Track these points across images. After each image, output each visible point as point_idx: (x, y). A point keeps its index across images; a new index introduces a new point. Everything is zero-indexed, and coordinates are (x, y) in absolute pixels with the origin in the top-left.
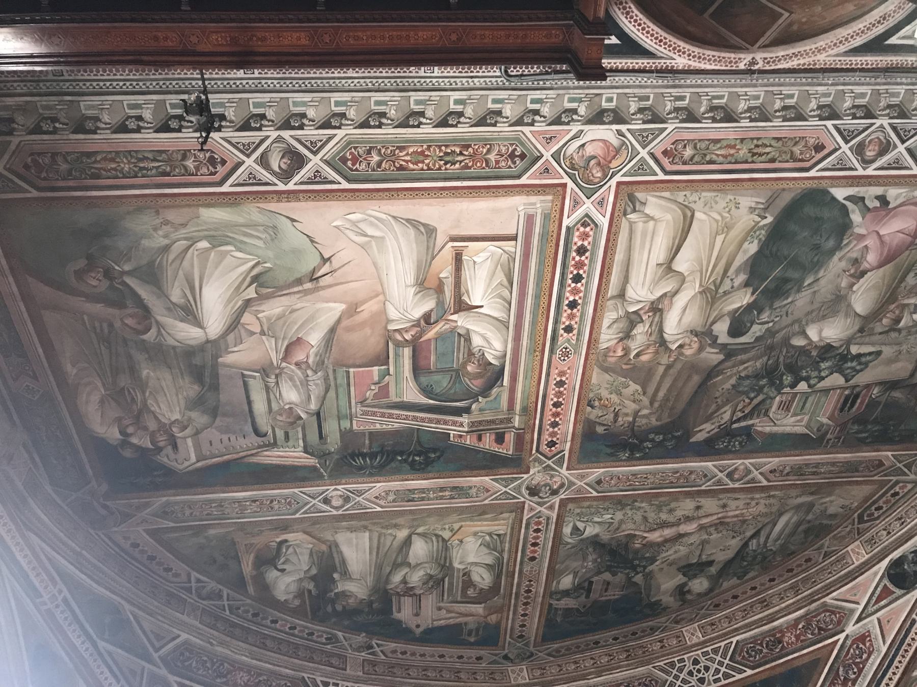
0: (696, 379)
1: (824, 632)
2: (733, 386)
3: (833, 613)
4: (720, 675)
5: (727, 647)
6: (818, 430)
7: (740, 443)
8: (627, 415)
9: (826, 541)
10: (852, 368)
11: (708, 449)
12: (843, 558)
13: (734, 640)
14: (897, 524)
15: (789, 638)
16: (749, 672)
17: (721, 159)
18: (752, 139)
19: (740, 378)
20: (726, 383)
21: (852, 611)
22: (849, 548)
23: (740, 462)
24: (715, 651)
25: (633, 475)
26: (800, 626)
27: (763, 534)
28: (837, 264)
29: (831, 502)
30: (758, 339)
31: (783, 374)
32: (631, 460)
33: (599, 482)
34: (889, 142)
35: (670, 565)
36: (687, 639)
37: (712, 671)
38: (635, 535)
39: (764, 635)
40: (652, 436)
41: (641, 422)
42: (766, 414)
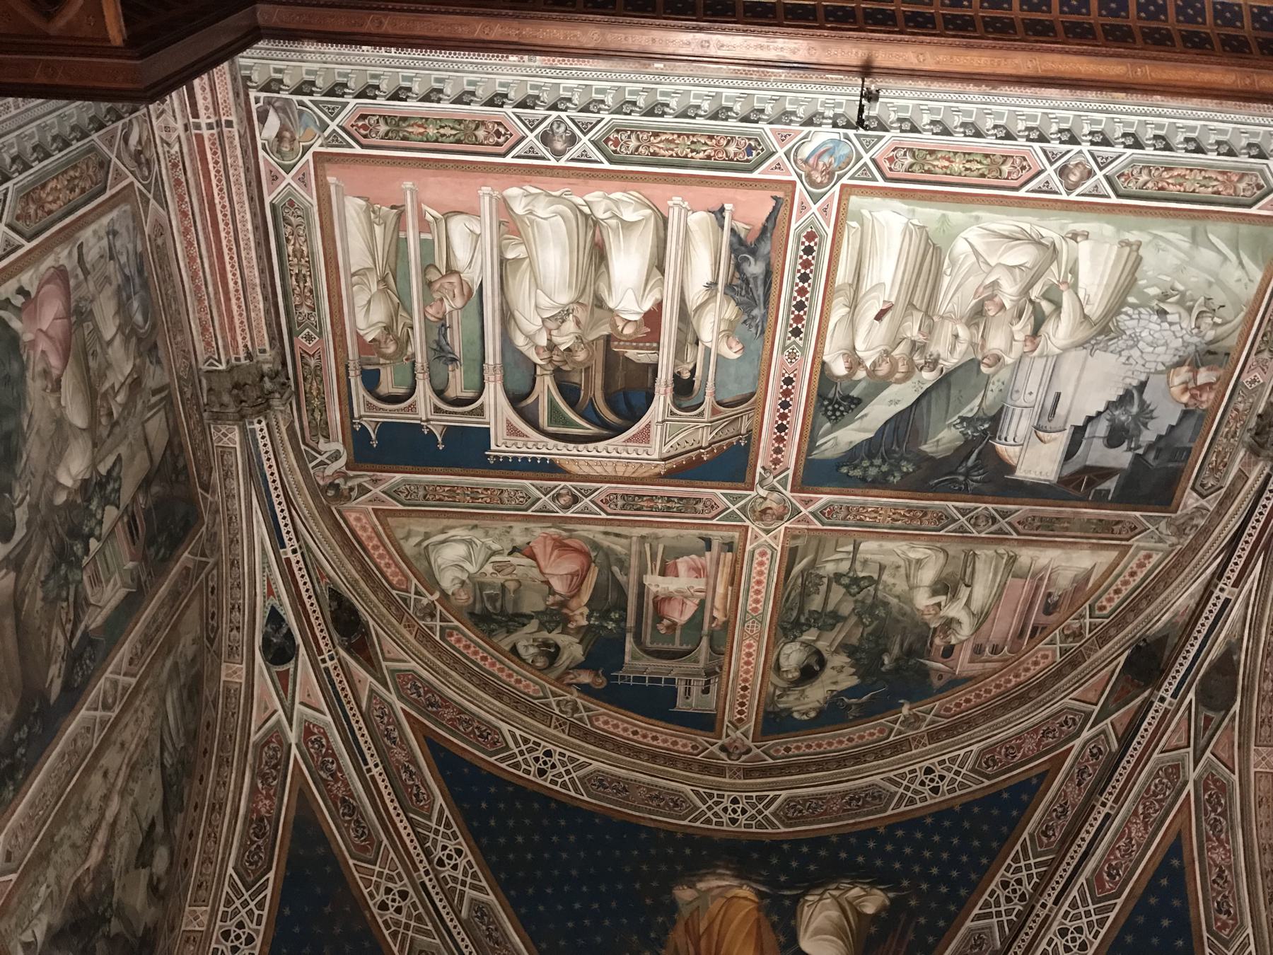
1: (280, 764)
2: (44, 599)
3: (268, 743)
4: (257, 912)
5: (233, 885)
6: (133, 580)
7: (90, 658)
10: (113, 489)
11: (73, 694)
13: (230, 871)
14: (236, 613)
15: (264, 806)
16: (271, 875)
19: (44, 583)
20: (35, 603)
21: (279, 722)
22: (223, 678)
23: (102, 680)
24: (229, 902)
26: (260, 786)
27: (166, 737)
28: (35, 386)
30: (29, 524)
32: (19, 790)
35: (127, 871)
36: (197, 928)
37: (247, 921)
38: (79, 879)
39: (245, 832)
42: (89, 604)
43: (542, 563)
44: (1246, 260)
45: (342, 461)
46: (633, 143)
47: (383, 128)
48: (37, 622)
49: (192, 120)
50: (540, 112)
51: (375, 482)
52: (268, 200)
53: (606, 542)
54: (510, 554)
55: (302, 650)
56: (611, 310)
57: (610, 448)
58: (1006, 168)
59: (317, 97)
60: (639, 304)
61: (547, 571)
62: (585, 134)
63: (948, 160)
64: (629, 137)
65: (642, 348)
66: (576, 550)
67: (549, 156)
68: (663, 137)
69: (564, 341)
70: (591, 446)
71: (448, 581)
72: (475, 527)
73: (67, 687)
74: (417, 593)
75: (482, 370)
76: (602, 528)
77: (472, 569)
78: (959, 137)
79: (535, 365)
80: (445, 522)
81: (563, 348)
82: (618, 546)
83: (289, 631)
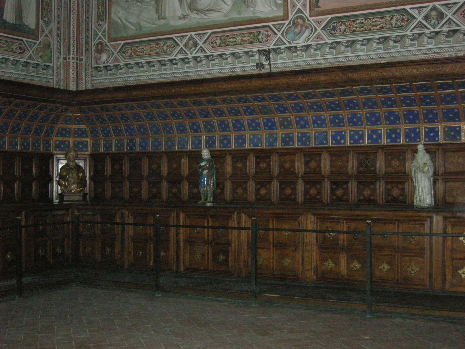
44: (119, 21)
46: (394, 21)
50: (445, 29)
58: (219, 41)
62: (420, 22)
63: (243, 41)
64: (396, 24)
67: (439, 7)
68: (378, 27)
78: (241, 51)
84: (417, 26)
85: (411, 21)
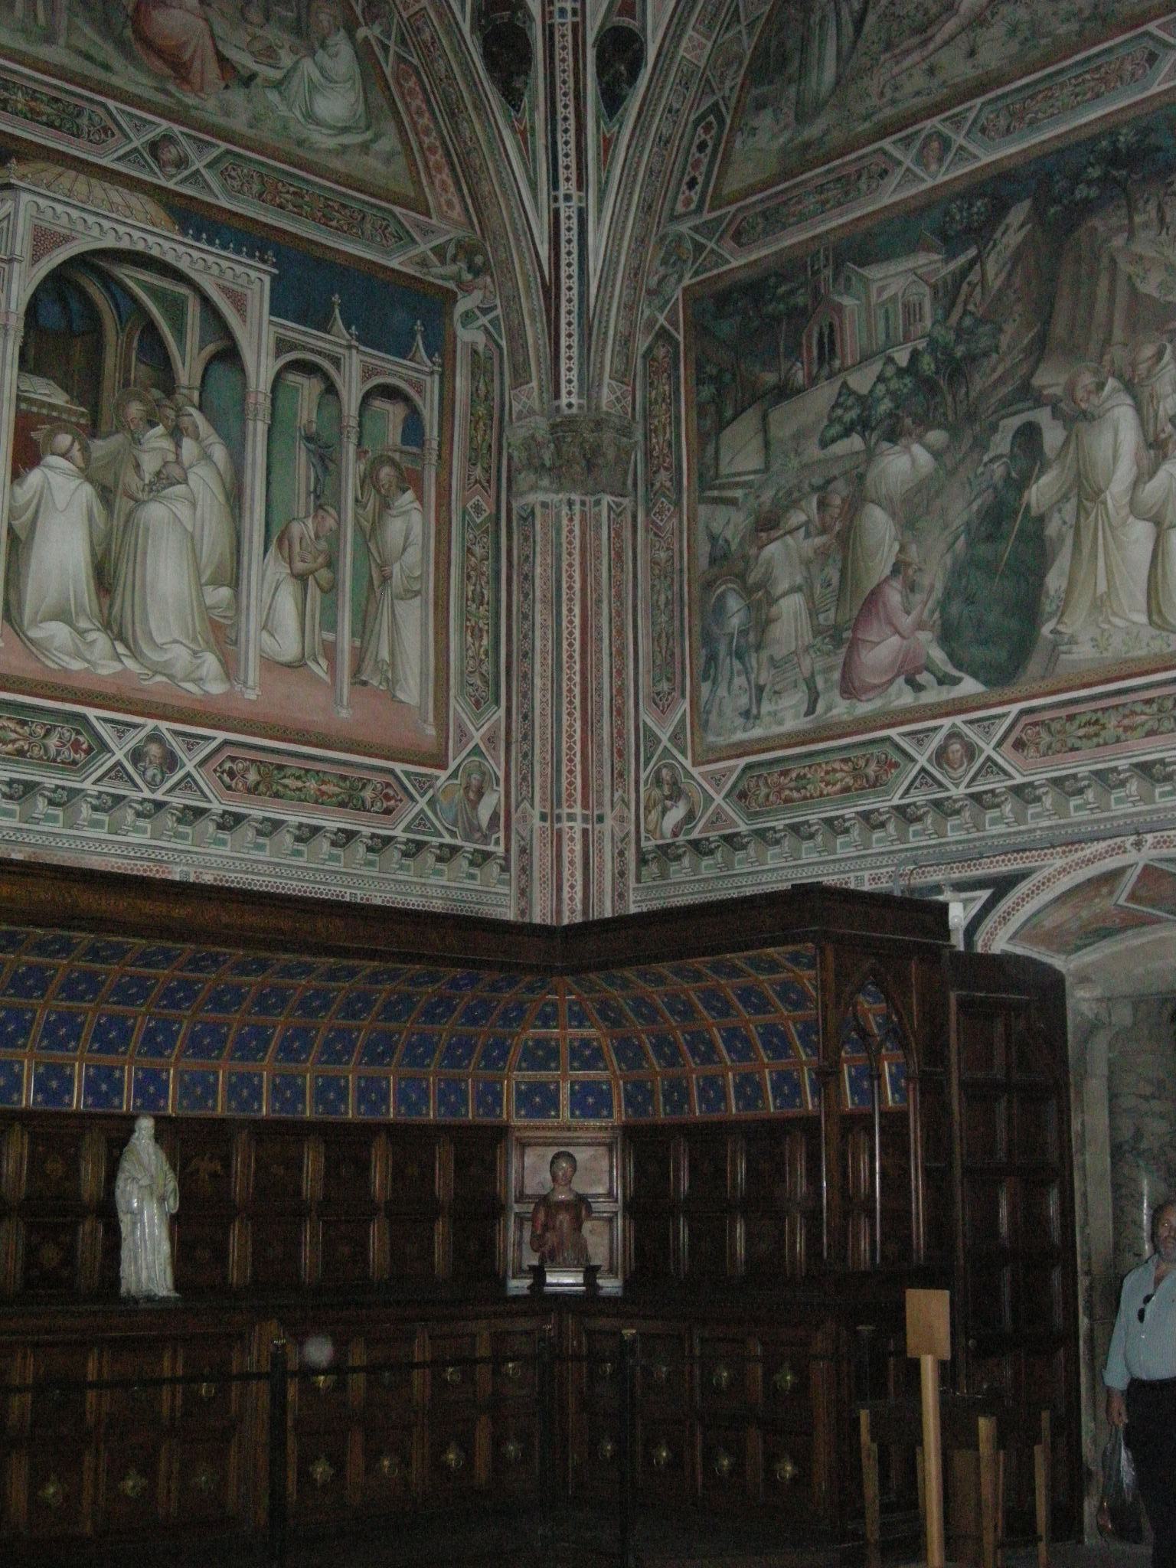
0: (1059, 329)
6: (848, 279)
7: (953, 219)
8: (1146, 225)
9: (748, 45)
10: (847, 409)
12: (710, 28)
14: (666, 132)
17: (1138, 708)
18: (1106, 744)
19: (997, 349)
20: (1014, 333)
22: (709, 45)
23: (941, 179)
25: (1098, 96)
27: (849, 29)
28: (934, 577)
29: (775, 136)
30: (994, 428)
31: (937, 373)
32: (1110, 128)
33: (1152, 58)
34: (940, 765)
40: (1094, 193)
41: (1118, 219)
42: (935, 288)
43: (208, 42)
45: (463, 305)
46: (53, 742)
47: (368, 794)
48: (1018, 308)
49: (590, 827)
50: (177, 800)
51: (423, 263)
52: (502, 712)
53: (107, 51)
54: (253, 76)
55: (591, 38)
56: (89, 479)
57: (96, 232)
59: (435, 841)
60: (46, 484)
61: (201, 24)
62: (119, 763)
64: (58, 753)
65: (43, 404)
66: (160, 53)
67: (168, 736)
68: (10, 747)
69: (156, 438)
70: (125, 244)
71: (342, 58)
72: (300, 143)
73: (1000, 208)
74: (385, 48)
75: (273, 415)
76: (116, 81)
77: (308, 66)
79: (201, 408)
80: (337, 164)
81: (160, 429)
82: (89, 36)
83: (600, 73)
84: (113, 774)
85: (99, 753)
